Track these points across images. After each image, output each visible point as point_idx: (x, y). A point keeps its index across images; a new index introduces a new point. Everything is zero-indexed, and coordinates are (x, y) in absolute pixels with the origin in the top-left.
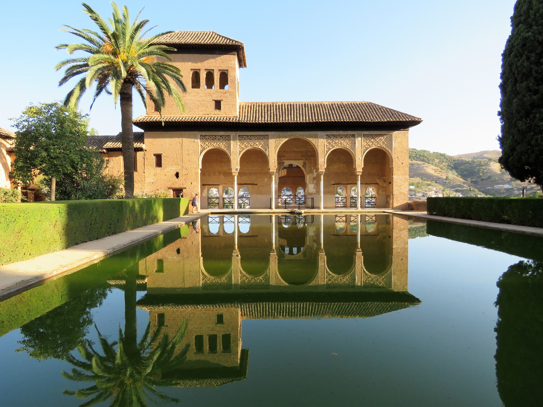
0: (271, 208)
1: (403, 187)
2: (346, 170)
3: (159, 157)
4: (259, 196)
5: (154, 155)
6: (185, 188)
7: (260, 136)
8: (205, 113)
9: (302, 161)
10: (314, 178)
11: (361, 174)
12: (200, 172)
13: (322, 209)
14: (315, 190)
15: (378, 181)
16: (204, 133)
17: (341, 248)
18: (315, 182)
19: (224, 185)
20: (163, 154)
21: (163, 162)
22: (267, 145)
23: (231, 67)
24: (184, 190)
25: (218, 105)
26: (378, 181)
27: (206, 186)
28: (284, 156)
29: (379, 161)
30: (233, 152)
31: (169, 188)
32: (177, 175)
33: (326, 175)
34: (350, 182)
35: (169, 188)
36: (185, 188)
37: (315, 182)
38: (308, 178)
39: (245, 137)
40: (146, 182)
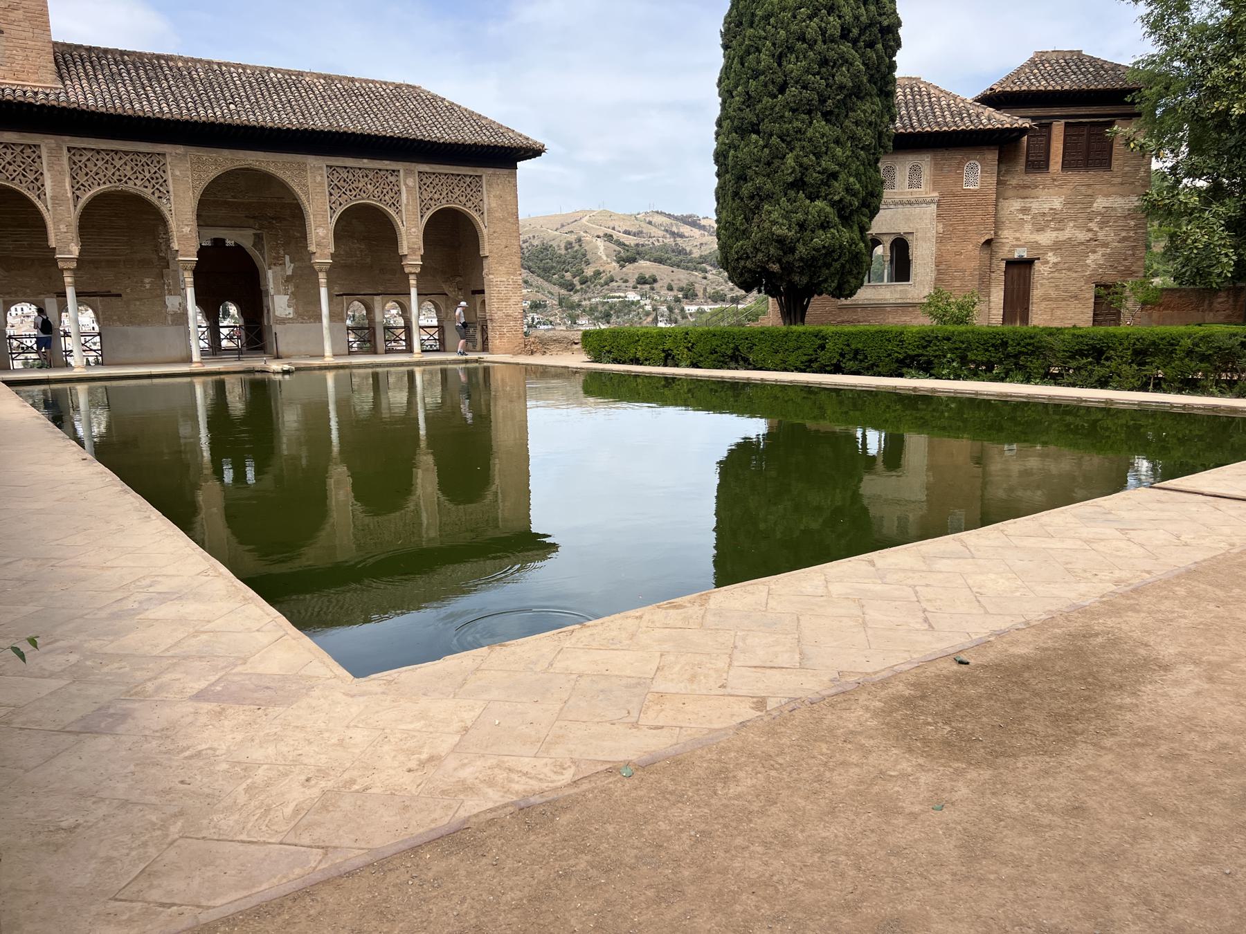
0: (189, 360)
1: (511, 302)
2: (368, 260)
4: (130, 329)
7: (138, 153)
9: (251, 232)
10: (288, 279)
13: (329, 360)
15: (446, 288)
17: (381, 450)
19: (7, 298)
22: (159, 182)
26: (446, 288)
29: (454, 242)
33: (331, 271)
34: (381, 289)
37: (291, 289)
38: (272, 278)
39: (89, 155)
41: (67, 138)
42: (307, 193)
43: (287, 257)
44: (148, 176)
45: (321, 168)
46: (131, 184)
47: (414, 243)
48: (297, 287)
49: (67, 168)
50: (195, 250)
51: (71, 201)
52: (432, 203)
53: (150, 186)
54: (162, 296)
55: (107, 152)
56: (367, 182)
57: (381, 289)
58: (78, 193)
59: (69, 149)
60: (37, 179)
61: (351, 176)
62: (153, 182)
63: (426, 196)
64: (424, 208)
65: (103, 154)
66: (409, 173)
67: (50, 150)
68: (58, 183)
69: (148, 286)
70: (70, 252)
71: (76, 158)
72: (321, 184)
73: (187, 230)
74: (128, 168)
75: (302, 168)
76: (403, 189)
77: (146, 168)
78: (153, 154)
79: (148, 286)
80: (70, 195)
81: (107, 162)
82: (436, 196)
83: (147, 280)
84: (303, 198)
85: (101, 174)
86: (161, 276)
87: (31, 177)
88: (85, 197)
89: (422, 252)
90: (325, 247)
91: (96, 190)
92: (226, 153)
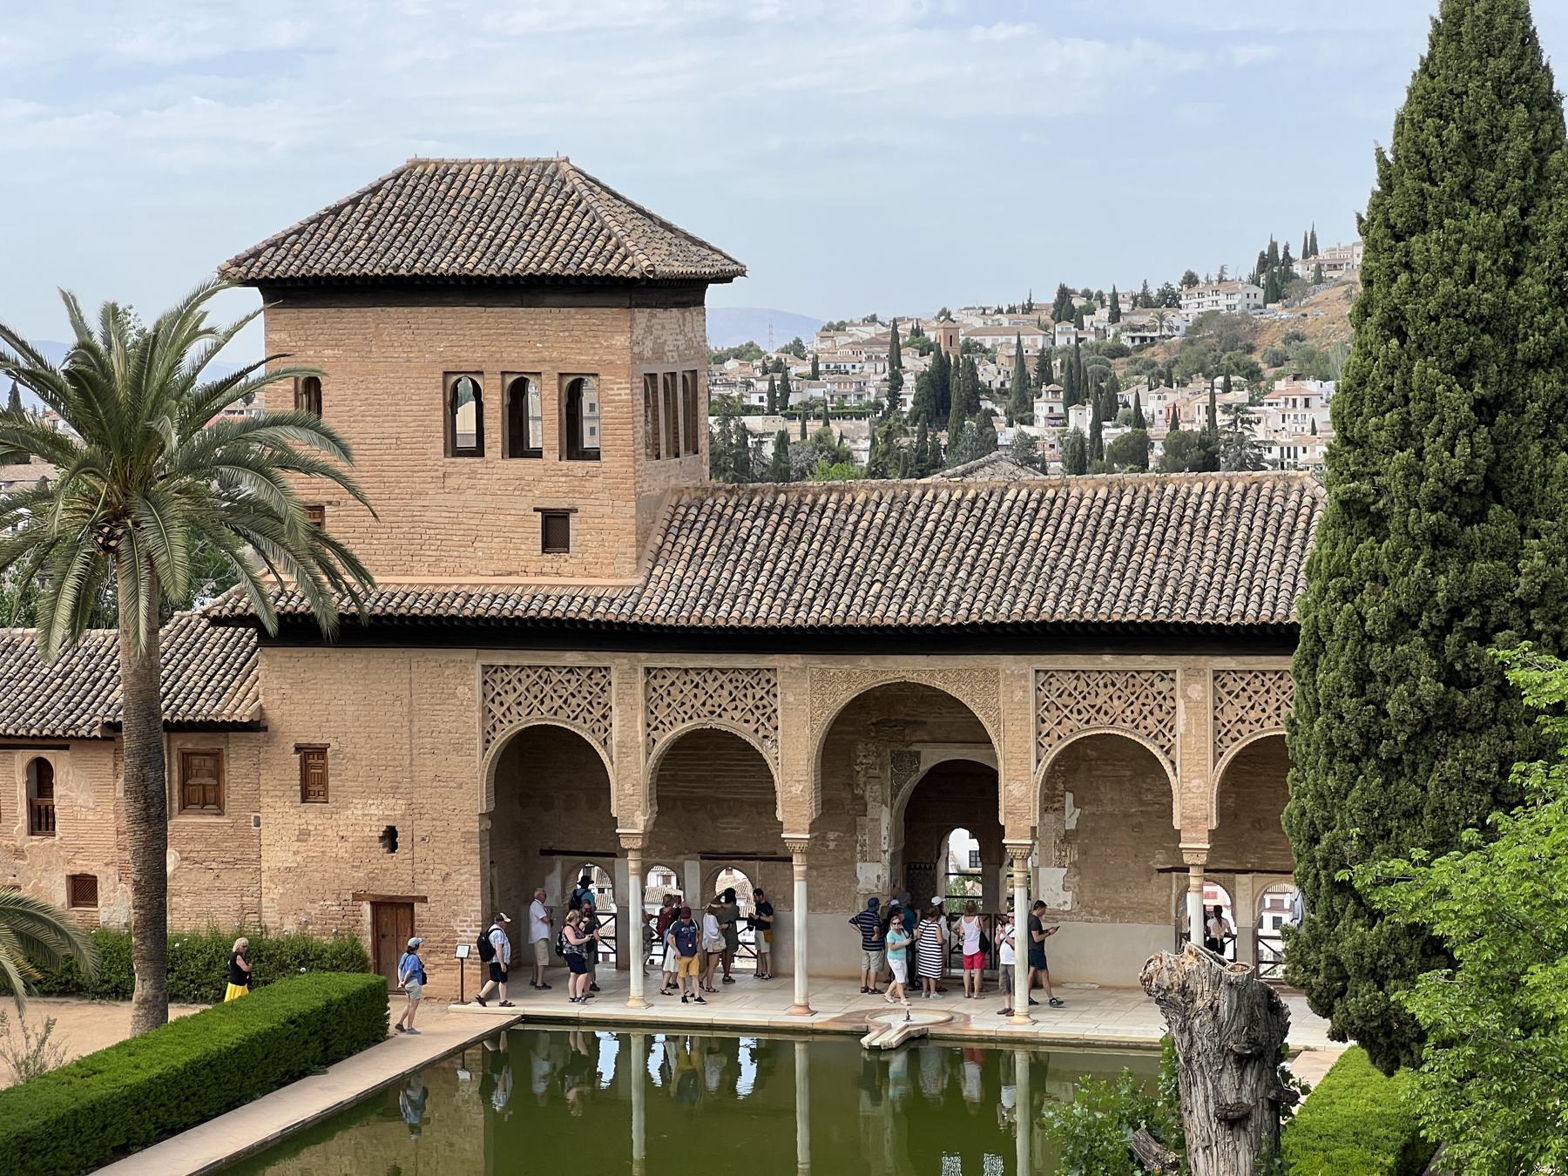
3: (312, 757)
5: (298, 749)
6: (424, 899)
7: (739, 670)
8: (502, 566)
10: (1067, 838)
11: (1203, 859)
12: (489, 824)
14: (1069, 896)
16: (499, 658)
18: (1073, 855)
20: (335, 746)
21: (332, 781)
23: (611, 362)
24: (417, 907)
25: (555, 529)
27: (559, 861)
28: (918, 724)
30: (621, 745)
31: (357, 897)
32: (390, 838)
34: (1252, 860)
35: (357, 897)
36: (424, 899)
37: (1073, 855)
39: (672, 676)
40: (264, 865)
41: (643, 656)
42: (997, 721)
43: (1069, 797)
44: (750, 702)
45: (1024, 676)
46: (726, 716)
47: (1195, 808)
48: (1083, 852)
49: (641, 699)
50: (806, 823)
51: (642, 750)
52: (1244, 728)
53: (753, 719)
54: (853, 862)
55: (698, 671)
56: (1106, 694)
57: (1252, 860)
58: (654, 734)
59: (648, 671)
60: (604, 717)
61: (1082, 686)
62: (757, 713)
63: (1231, 713)
64: (1220, 736)
65: (693, 675)
66: (1192, 674)
67: (622, 672)
68: (628, 723)
69: (832, 845)
70: (634, 825)
71: (655, 683)
72: (1022, 704)
73: (797, 789)
74: (725, 693)
75: (991, 677)
76: (1180, 704)
77: (750, 692)
78: (760, 670)
79: (832, 845)
80: (641, 739)
81: (697, 686)
82: (1253, 715)
83: (831, 836)
84: (990, 731)
85: (689, 704)
86: (853, 829)
87: (597, 714)
88: (664, 739)
89: (1214, 825)
90: (1022, 817)
91: (681, 728)
92: (867, 662)
